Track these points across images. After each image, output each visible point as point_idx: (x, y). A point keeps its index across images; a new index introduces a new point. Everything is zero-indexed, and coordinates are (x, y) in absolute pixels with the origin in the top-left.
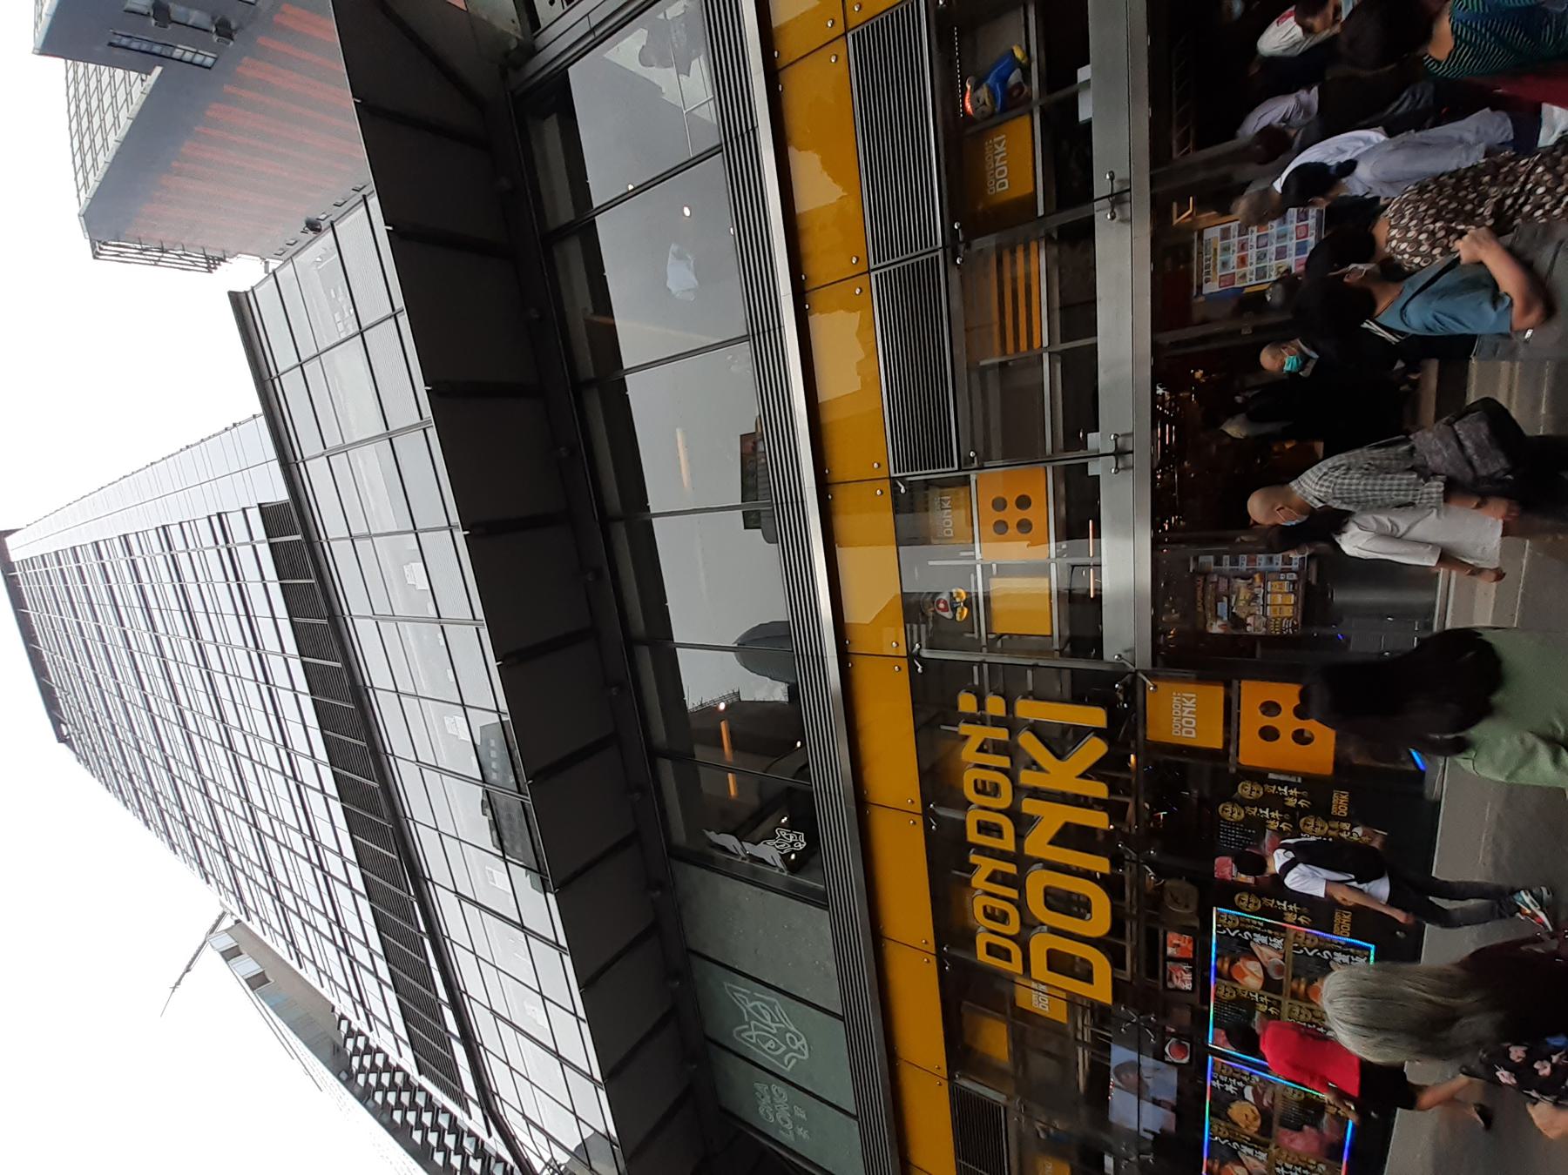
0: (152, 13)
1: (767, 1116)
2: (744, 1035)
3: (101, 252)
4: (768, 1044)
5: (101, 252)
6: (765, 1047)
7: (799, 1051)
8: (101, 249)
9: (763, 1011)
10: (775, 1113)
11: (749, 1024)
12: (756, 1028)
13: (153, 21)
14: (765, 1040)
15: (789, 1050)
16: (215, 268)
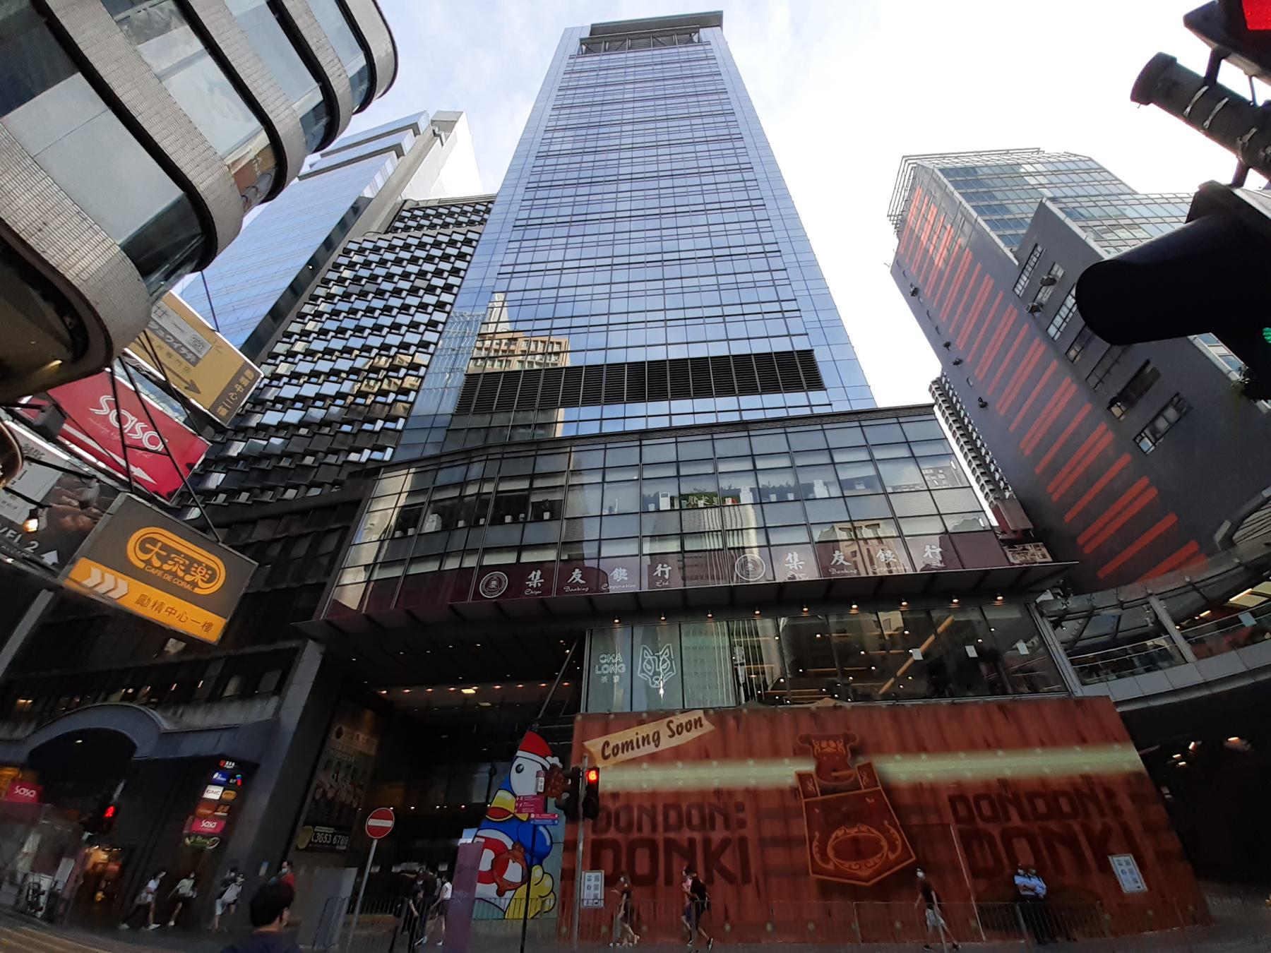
0: (1050, 277)
1: (603, 659)
2: (645, 651)
3: (907, 164)
4: (648, 666)
5: (907, 164)
6: (645, 663)
7: (653, 683)
8: (909, 164)
9: (666, 664)
10: (607, 663)
11: (654, 655)
12: (654, 660)
13: (1045, 278)
14: (649, 662)
15: (652, 677)
16: (895, 228)
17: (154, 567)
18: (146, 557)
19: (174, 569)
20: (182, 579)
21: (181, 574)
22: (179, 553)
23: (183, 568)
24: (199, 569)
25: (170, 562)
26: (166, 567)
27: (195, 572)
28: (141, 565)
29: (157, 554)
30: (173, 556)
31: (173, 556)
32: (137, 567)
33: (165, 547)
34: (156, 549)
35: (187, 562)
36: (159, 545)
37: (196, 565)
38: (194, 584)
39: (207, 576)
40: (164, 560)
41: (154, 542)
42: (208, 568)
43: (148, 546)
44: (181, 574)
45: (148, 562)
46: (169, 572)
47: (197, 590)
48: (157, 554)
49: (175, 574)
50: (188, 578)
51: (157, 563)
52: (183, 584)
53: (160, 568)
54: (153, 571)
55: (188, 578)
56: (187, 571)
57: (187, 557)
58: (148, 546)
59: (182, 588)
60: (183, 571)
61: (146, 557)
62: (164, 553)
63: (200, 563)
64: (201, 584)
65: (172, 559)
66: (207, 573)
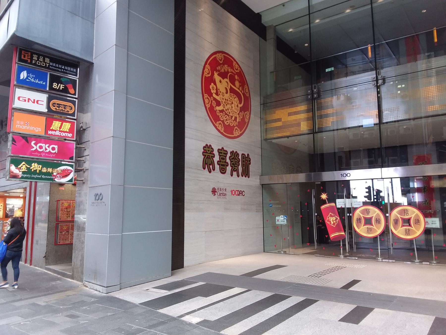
17: (57, 110)
18: (55, 108)
19: (62, 109)
20: (65, 111)
21: (64, 110)
22: (61, 105)
23: (64, 108)
24: (67, 107)
25: (60, 107)
26: (60, 109)
27: (67, 108)
28: (55, 110)
29: (57, 106)
30: (60, 106)
31: (60, 106)
32: (54, 111)
33: (58, 104)
34: (56, 105)
35: (64, 106)
36: (56, 104)
37: (66, 106)
38: (68, 111)
39: (70, 108)
40: (59, 107)
41: (55, 104)
42: (69, 106)
43: (54, 105)
44: (64, 110)
45: (56, 109)
46: (61, 110)
47: (69, 113)
48: (57, 106)
49: (62, 110)
50: (66, 110)
51: (58, 108)
52: (65, 112)
53: (59, 110)
54: (58, 111)
55: (66, 110)
56: (65, 109)
57: (63, 105)
58: (54, 105)
59: (65, 113)
60: (64, 109)
61: (55, 108)
62: (58, 106)
63: (67, 106)
64: (69, 111)
65: (60, 107)
66: (70, 108)
